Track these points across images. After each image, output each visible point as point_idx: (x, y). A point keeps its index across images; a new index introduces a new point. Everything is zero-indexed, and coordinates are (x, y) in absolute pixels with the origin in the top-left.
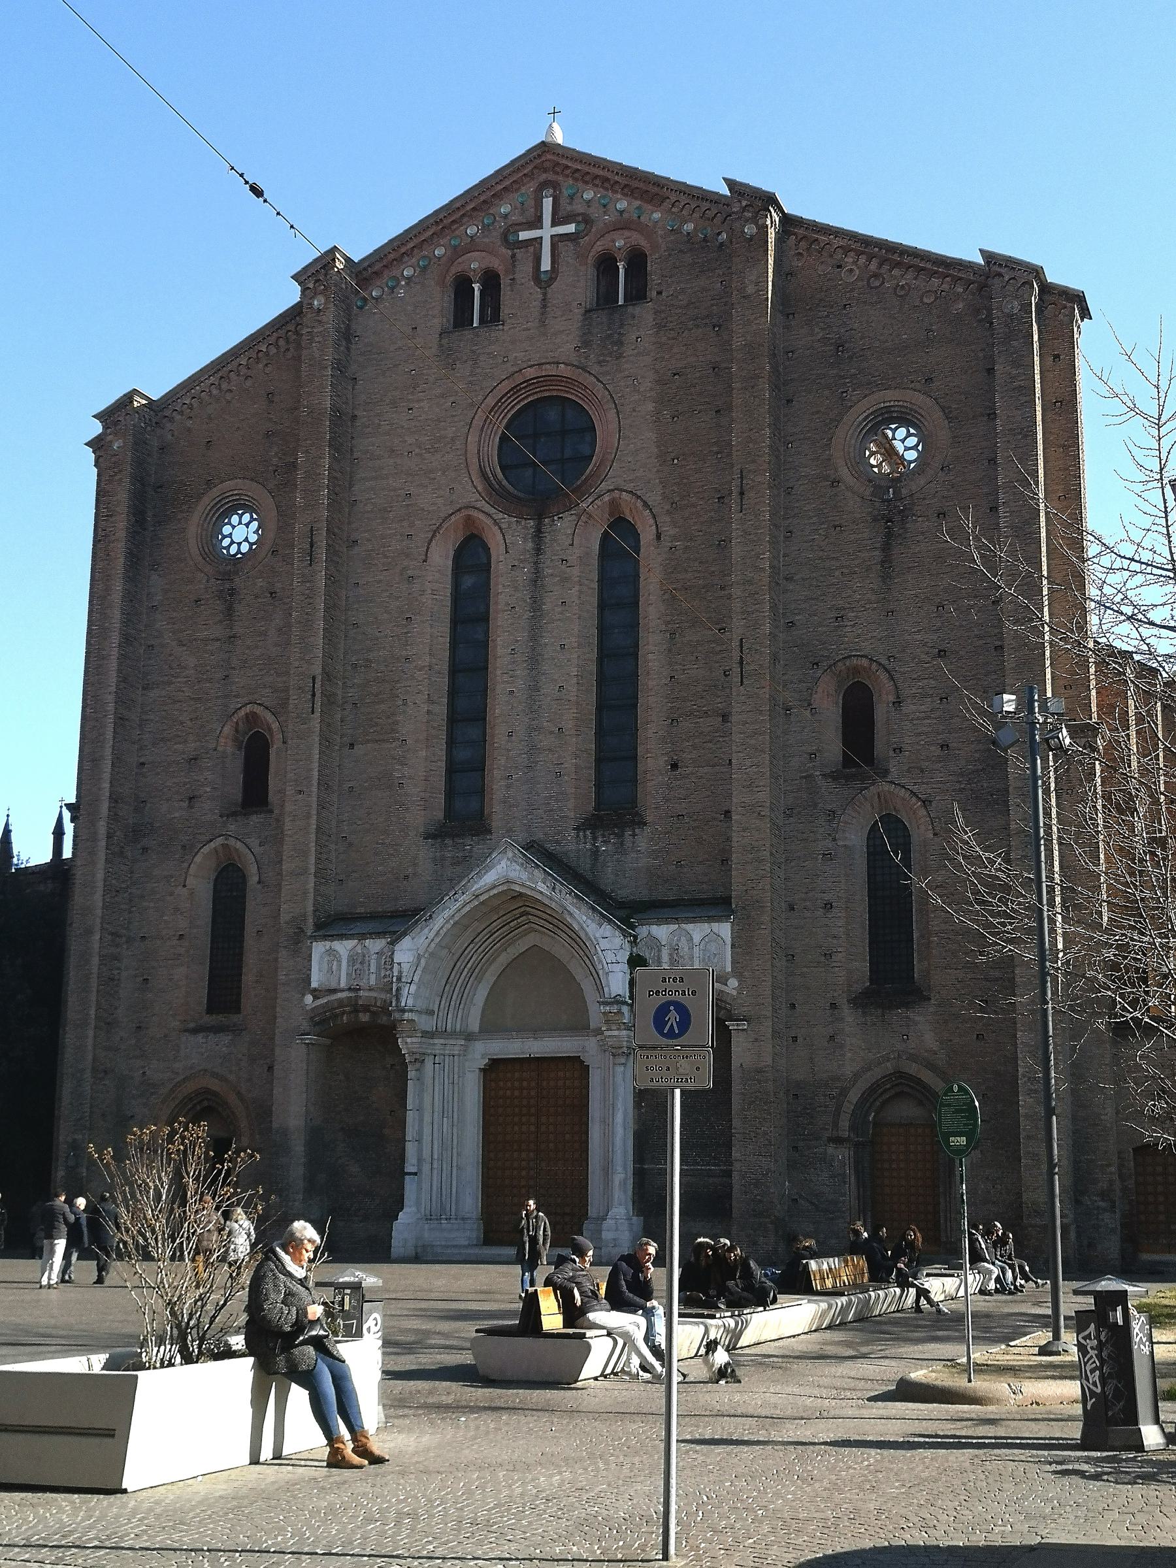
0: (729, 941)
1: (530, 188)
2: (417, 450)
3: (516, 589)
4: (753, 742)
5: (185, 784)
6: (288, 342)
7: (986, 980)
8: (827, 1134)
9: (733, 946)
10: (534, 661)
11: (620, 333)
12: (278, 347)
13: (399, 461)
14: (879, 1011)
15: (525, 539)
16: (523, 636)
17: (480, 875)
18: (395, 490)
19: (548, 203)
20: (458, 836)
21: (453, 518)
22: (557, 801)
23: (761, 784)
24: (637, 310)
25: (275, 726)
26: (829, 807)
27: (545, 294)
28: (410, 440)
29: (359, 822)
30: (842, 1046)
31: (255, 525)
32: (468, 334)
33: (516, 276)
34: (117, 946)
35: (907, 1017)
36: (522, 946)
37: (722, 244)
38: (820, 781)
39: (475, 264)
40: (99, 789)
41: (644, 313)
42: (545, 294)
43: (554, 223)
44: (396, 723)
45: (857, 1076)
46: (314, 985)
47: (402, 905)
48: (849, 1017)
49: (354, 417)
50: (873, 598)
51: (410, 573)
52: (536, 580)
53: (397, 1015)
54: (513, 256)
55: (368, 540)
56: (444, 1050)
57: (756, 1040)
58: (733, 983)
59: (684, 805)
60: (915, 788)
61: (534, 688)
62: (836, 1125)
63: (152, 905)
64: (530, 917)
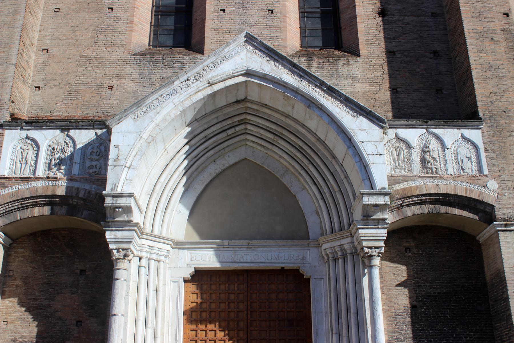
9: (486, 150)
17: (215, 65)
23: (489, 16)
29: (64, 38)
36: (232, 159)
56: (151, 253)
58: (493, 185)
59: (394, 44)
64: (249, 127)
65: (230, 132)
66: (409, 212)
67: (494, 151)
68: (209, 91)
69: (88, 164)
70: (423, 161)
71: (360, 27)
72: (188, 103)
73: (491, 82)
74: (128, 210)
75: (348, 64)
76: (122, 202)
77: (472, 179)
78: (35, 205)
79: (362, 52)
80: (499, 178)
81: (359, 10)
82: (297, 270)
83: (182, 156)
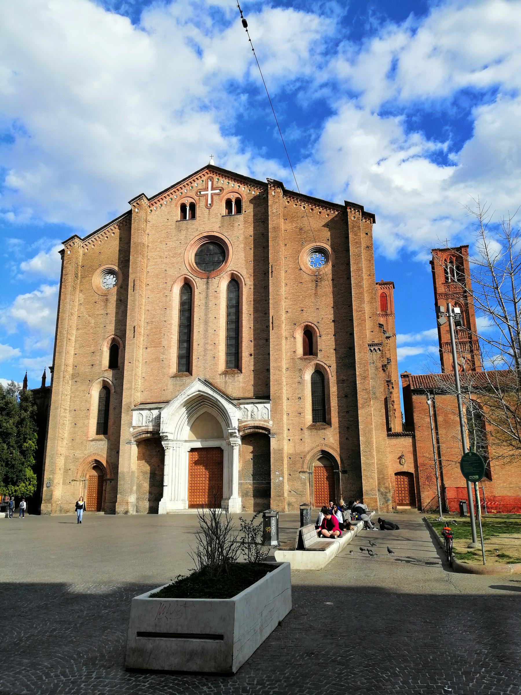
0: (269, 410)
1: (204, 178)
2: (169, 257)
3: (200, 300)
4: (277, 347)
5: (90, 360)
6: (126, 222)
7: (349, 421)
8: (300, 470)
9: (271, 411)
10: (206, 323)
11: (233, 223)
12: (123, 224)
13: (163, 260)
14: (316, 431)
15: (203, 285)
16: (202, 314)
18: (161, 269)
19: (210, 183)
20: (181, 377)
21: (180, 278)
22: (213, 366)
24: (238, 216)
25: (121, 342)
26: (299, 368)
27: (209, 211)
28: (166, 253)
30: (304, 442)
31: (115, 279)
32: (185, 222)
33: (200, 205)
34: (66, 413)
35: (325, 433)
37: (264, 198)
38: (297, 360)
39: (187, 201)
40: (61, 362)
41: (241, 217)
42: (209, 211)
43: (212, 189)
44: (161, 341)
45: (308, 452)
46: (134, 425)
47: (163, 399)
48: (307, 433)
49: (148, 246)
50: (312, 304)
51: (166, 294)
52: (207, 296)
53: (161, 435)
54: (199, 199)
55: (152, 284)
57: (278, 440)
58: (271, 422)
60: (326, 362)
61: (206, 330)
62: (302, 467)
63: (78, 399)
65: (199, 405)
66: (247, 431)
67: (273, 411)
68: (188, 398)
69: (157, 421)
70: (251, 415)
71: (243, 361)
72: (182, 402)
73: (276, 386)
74: (167, 436)
75: (238, 377)
76: (165, 434)
77: (265, 421)
78: (143, 434)
79: (243, 371)
80: (273, 420)
81: (243, 354)
82: (220, 447)
83: (185, 413)
